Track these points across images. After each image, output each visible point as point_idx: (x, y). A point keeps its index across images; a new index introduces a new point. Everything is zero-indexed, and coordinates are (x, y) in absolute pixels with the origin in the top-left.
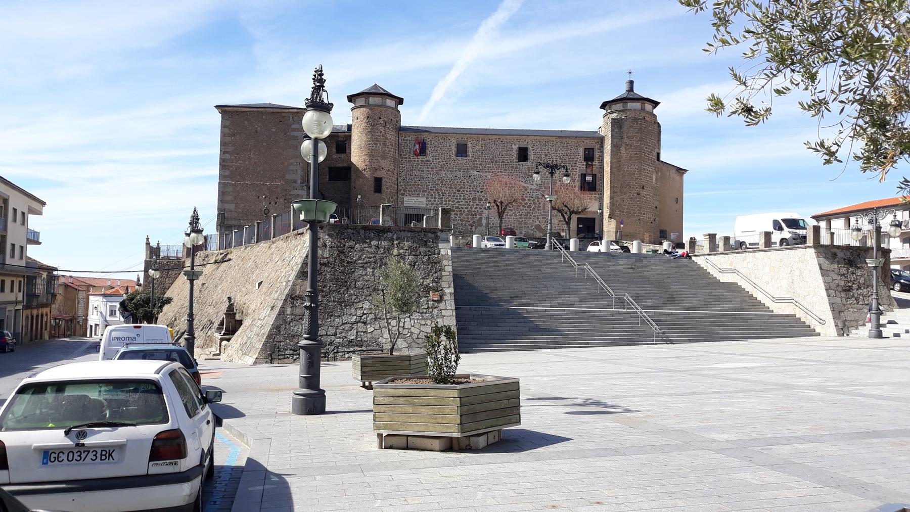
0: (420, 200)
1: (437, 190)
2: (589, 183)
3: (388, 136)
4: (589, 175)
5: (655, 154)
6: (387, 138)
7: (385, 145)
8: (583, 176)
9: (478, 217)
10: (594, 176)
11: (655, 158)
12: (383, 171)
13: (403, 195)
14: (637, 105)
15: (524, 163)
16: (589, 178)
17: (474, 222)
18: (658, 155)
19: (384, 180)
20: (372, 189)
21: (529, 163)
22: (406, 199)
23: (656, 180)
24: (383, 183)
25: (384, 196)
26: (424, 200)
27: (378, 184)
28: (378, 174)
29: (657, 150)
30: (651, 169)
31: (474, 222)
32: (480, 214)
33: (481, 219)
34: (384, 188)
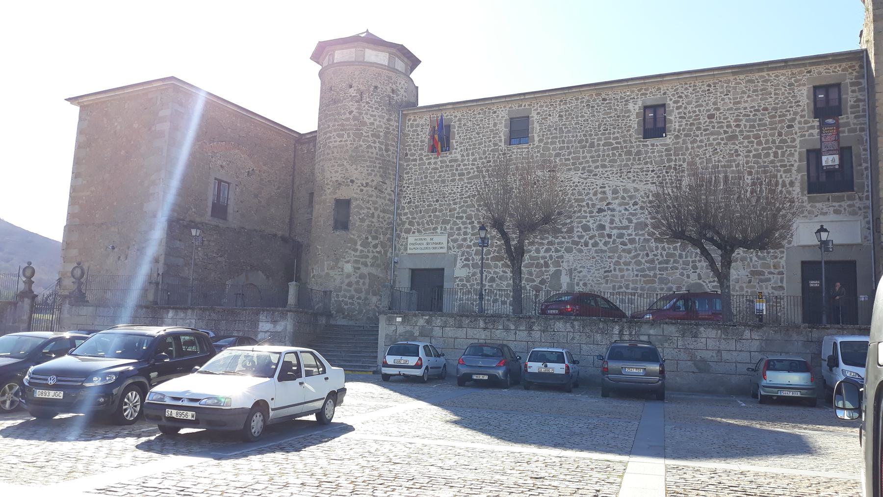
0: (436, 239)
1: (469, 217)
2: (830, 171)
3: (367, 119)
4: (830, 152)
6: (364, 124)
7: (359, 136)
8: (813, 155)
9: (552, 269)
10: (845, 152)
12: (355, 186)
13: (408, 231)
15: (657, 141)
16: (830, 160)
17: (543, 282)
19: (354, 204)
20: (331, 222)
21: (669, 139)
22: (411, 239)
25: (353, 234)
26: (443, 239)
28: (344, 193)
31: (543, 282)
32: (557, 264)
33: (557, 274)
34: (354, 219)
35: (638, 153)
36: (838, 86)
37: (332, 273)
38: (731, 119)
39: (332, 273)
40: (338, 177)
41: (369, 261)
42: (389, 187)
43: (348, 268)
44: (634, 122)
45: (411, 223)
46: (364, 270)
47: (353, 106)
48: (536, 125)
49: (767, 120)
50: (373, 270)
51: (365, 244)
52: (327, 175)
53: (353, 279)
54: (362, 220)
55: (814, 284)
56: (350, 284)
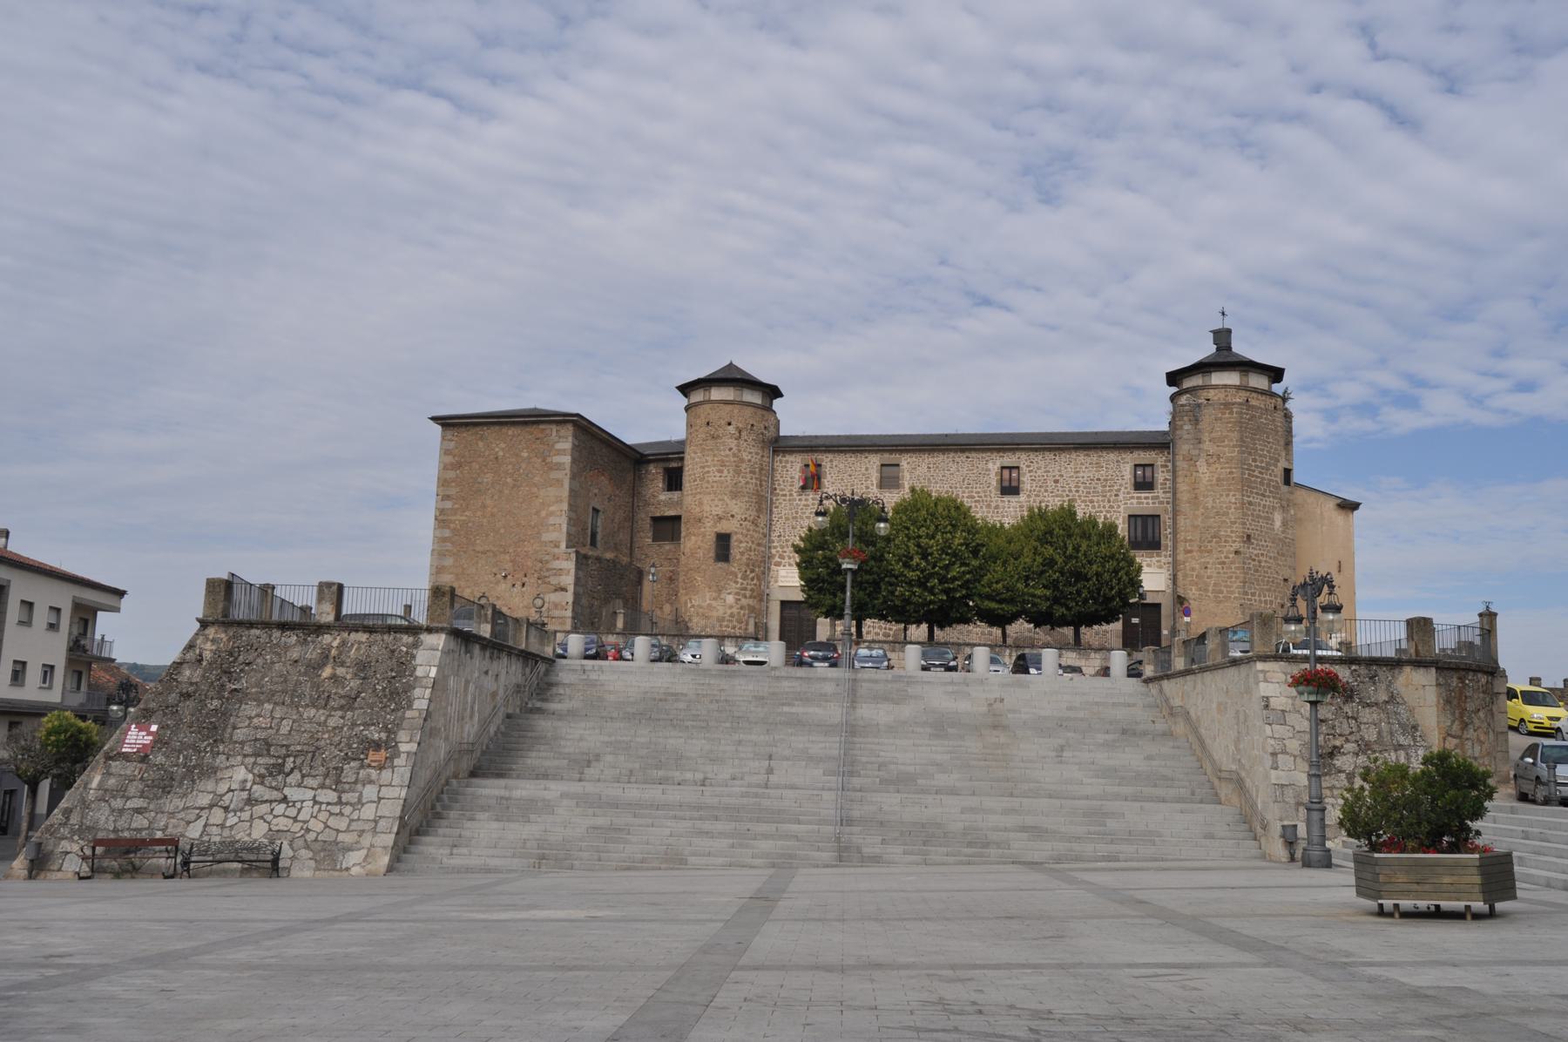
3: (745, 456)
5: (1279, 471)
6: (742, 461)
11: (1280, 479)
13: (778, 564)
14: (1232, 378)
15: (1013, 499)
18: (1287, 473)
19: (734, 538)
20: (712, 554)
21: (1022, 497)
23: (1285, 523)
24: (733, 542)
25: (734, 567)
27: (723, 545)
28: (724, 527)
29: (1283, 464)
30: (1268, 502)
35: (997, 507)
36: (1152, 465)
37: (714, 603)
38: (1072, 485)
39: (714, 603)
40: (719, 511)
41: (748, 593)
42: (762, 521)
43: (730, 599)
44: (994, 481)
45: (781, 557)
46: (744, 602)
47: (733, 443)
48: (907, 475)
49: (1100, 489)
50: (751, 602)
51: (745, 577)
52: (707, 508)
53: (735, 610)
54: (742, 554)
55: (1135, 620)
56: (732, 615)
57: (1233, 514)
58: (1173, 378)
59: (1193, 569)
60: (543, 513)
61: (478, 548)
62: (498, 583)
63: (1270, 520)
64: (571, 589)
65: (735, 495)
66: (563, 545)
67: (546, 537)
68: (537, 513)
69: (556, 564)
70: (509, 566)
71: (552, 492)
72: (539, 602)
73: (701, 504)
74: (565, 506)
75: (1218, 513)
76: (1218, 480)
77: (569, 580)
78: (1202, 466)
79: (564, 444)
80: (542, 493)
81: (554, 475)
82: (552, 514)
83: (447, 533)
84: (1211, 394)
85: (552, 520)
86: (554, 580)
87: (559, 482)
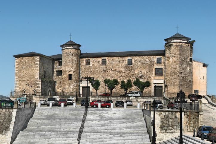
3: (74, 59)
5: (189, 59)
47: (71, 57)
52: (67, 69)
57: (178, 68)
58: (166, 40)
59: (168, 79)
60: (35, 73)
61: (23, 80)
62: (27, 86)
63: (186, 69)
64: (41, 87)
65: (72, 67)
66: (39, 79)
67: (36, 77)
68: (34, 73)
69: (38, 82)
70: (29, 83)
71: (36, 69)
72: (34, 91)
73: (65, 69)
74: (39, 71)
75: (174, 68)
76: (175, 61)
77: (40, 85)
78: (171, 58)
79: (38, 59)
80: (34, 69)
81: (36, 65)
82: (36, 73)
83: (17, 77)
84: (173, 44)
85: (36, 74)
86: (37, 85)
87: (37, 67)
